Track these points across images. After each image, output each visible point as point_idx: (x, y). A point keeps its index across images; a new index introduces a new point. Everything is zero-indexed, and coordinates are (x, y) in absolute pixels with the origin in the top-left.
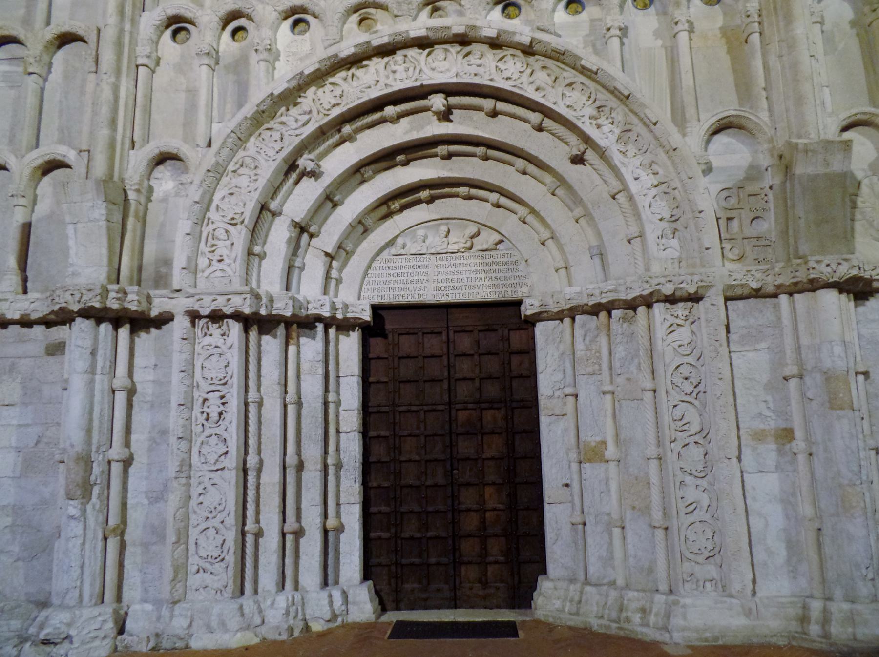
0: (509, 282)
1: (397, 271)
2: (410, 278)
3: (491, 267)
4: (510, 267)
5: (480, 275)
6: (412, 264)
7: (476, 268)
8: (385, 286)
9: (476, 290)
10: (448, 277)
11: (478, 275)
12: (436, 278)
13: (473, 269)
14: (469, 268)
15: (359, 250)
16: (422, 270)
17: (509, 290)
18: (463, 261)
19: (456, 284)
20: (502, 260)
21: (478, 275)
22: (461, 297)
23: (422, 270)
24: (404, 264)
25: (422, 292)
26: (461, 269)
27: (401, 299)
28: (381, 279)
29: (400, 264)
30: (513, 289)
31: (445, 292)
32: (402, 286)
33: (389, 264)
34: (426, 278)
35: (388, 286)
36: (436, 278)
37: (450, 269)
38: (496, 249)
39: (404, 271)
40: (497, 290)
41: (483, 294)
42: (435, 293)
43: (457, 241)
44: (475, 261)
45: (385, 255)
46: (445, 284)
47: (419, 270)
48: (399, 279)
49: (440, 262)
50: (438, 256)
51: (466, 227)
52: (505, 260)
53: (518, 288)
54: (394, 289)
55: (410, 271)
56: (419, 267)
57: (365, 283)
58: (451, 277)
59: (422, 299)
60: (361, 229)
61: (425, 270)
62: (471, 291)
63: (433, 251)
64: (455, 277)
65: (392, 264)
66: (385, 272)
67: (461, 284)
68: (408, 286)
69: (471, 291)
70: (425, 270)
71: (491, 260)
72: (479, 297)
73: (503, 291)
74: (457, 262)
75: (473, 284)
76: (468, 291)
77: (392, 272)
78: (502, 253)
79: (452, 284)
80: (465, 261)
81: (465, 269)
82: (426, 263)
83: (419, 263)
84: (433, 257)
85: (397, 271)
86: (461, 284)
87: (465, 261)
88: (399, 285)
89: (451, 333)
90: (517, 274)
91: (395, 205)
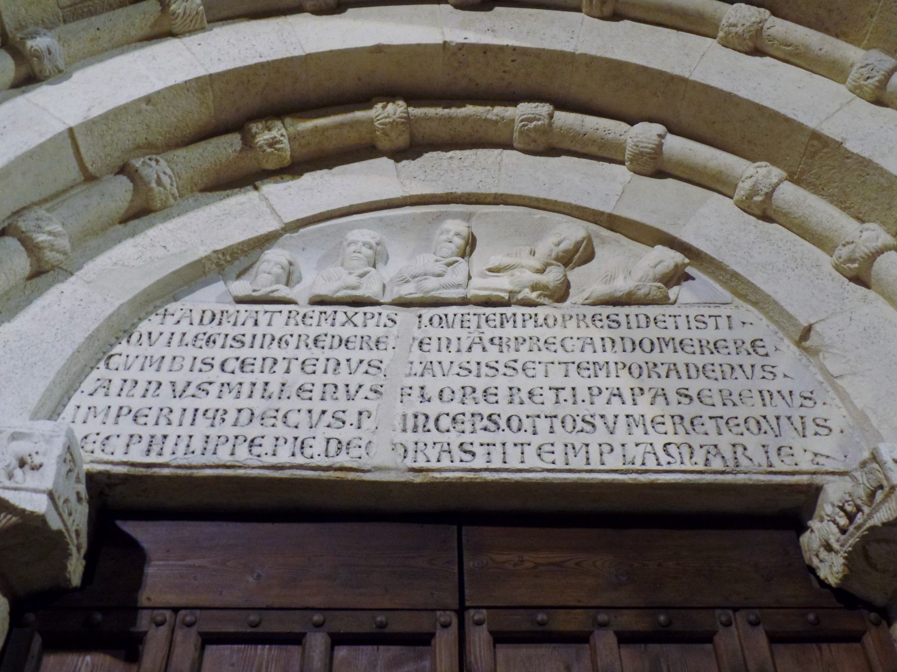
0: (742, 412)
1: (245, 353)
2: (297, 378)
3: (656, 357)
4: (735, 360)
5: (613, 382)
6: (313, 332)
7: (589, 356)
8: (177, 405)
9: (601, 434)
10: (471, 381)
11: (602, 381)
12: (416, 382)
13: (578, 357)
14: (562, 356)
15: (92, 268)
16: (356, 355)
17: (752, 441)
18: (530, 330)
19: (504, 410)
20: (696, 334)
21: (602, 381)
22: (532, 461)
23: (356, 355)
24: (278, 329)
25: (346, 434)
26: (524, 356)
27: (242, 453)
28: (165, 377)
29: (259, 331)
30: (770, 439)
31: (454, 438)
32: (258, 404)
33: (212, 329)
34: (368, 381)
35: (189, 403)
36: (416, 382)
37: (477, 354)
38: (664, 301)
39: (275, 351)
40: (696, 440)
41: (636, 454)
42: (409, 438)
43: (513, 258)
44: (584, 332)
45: (210, 297)
46: (455, 408)
47: (341, 354)
48: (247, 378)
49: (435, 332)
50: (427, 313)
51: (538, 233)
52: (710, 334)
53: (789, 437)
54: (218, 416)
55: (303, 354)
56: (345, 343)
57: (89, 384)
58: (481, 384)
59: (343, 459)
60: (119, 192)
61: (366, 355)
62: (578, 440)
63: (408, 290)
64: (502, 383)
65: (227, 328)
66: (190, 352)
67: (530, 408)
68: (284, 406)
69: (578, 440)
70: (366, 355)
71: (653, 332)
72: (614, 461)
73: (725, 442)
74: (509, 332)
75: (583, 410)
76: (561, 436)
77: (218, 353)
78: (693, 312)
79: (485, 409)
80: (543, 333)
81: (546, 356)
82: (373, 331)
83: (347, 332)
84: (406, 316)
85: (245, 353)
86: (530, 408)
87: (543, 333)
88: (243, 402)
89: (479, 638)
90: (774, 386)
91: (276, 137)
